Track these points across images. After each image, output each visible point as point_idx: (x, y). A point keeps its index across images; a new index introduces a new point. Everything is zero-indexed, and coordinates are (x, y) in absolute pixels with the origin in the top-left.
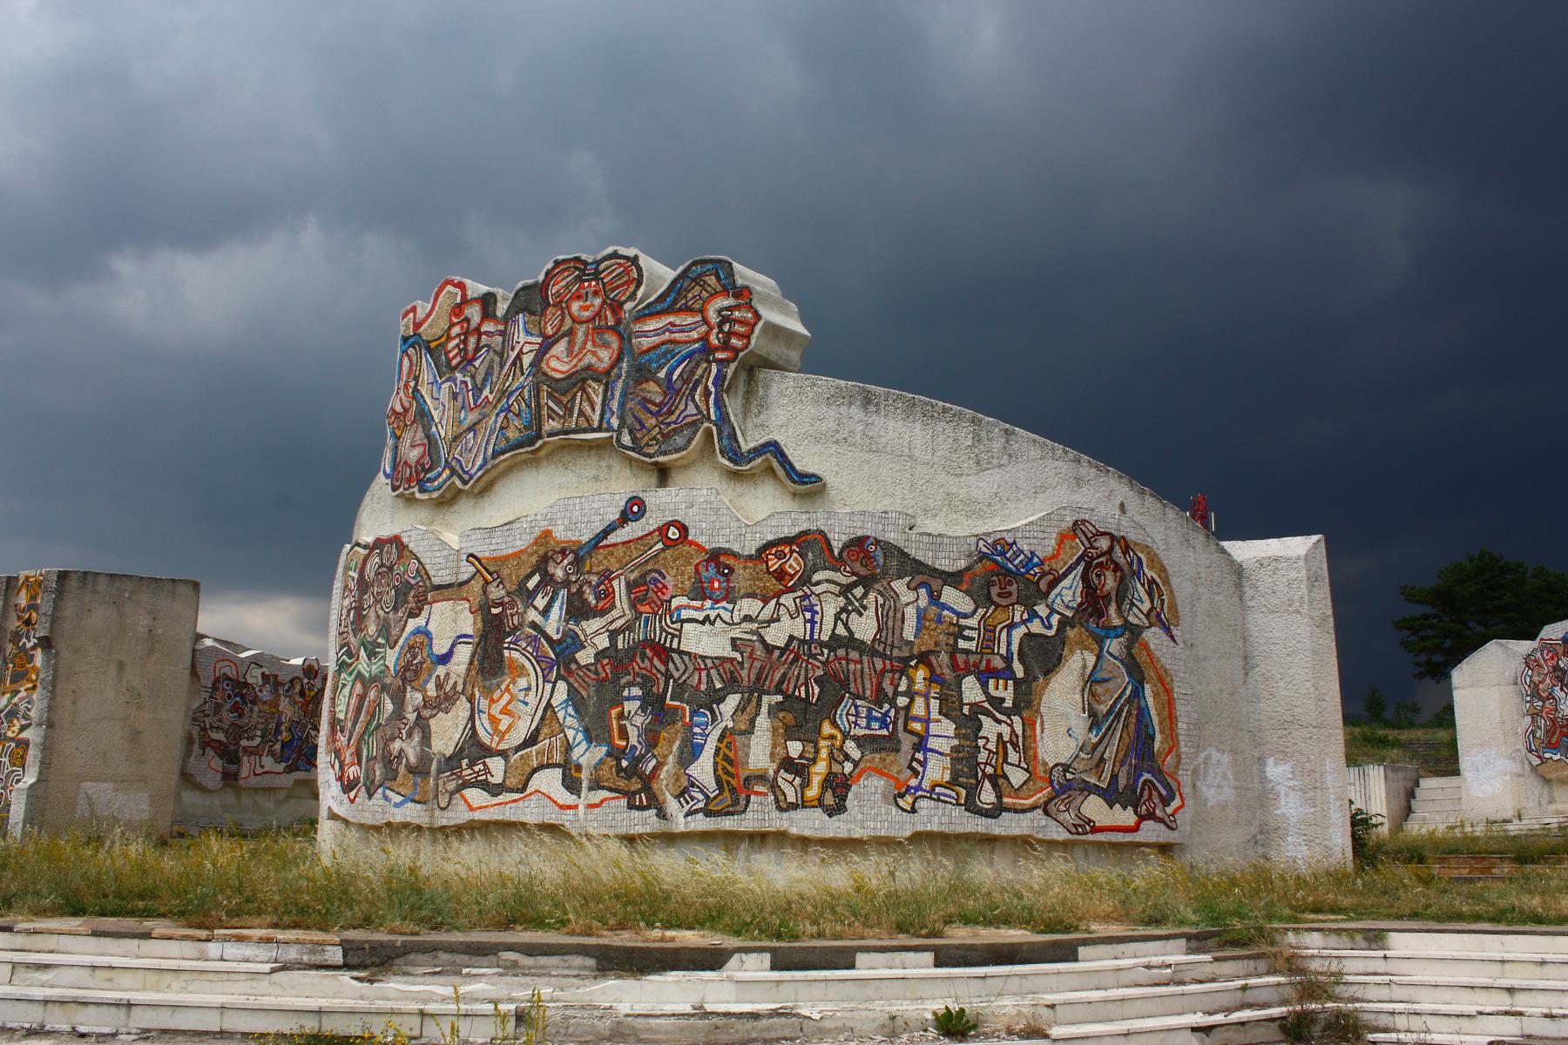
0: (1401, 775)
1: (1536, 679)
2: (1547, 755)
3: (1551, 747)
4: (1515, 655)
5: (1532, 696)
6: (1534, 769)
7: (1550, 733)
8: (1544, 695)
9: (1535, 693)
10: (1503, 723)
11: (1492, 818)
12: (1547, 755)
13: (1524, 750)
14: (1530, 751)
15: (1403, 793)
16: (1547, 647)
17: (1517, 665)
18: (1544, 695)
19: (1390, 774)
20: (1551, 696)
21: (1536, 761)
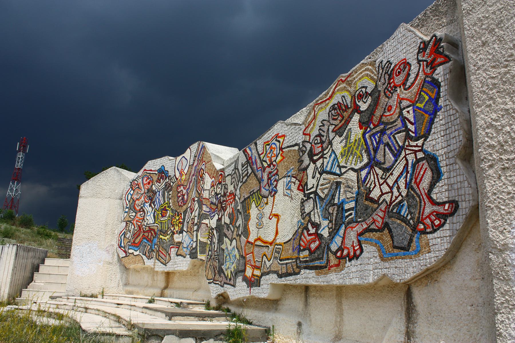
0: (31, 254)
1: (135, 197)
2: (131, 251)
3: (135, 245)
4: (125, 179)
5: (130, 209)
6: (120, 259)
7: (135, 235)
8: (138, 208)
9: (132, 207)
10: (106, 225)
11: (84, 293)
12: (131, 251)
13: (116, 246)
14: (120, 247)
15: (29, 267)
16: (148, 176)
17: (125, 186)
18: (138, 208)
19: (21, 253)
20: (142, 210)
21: (122, 254)
